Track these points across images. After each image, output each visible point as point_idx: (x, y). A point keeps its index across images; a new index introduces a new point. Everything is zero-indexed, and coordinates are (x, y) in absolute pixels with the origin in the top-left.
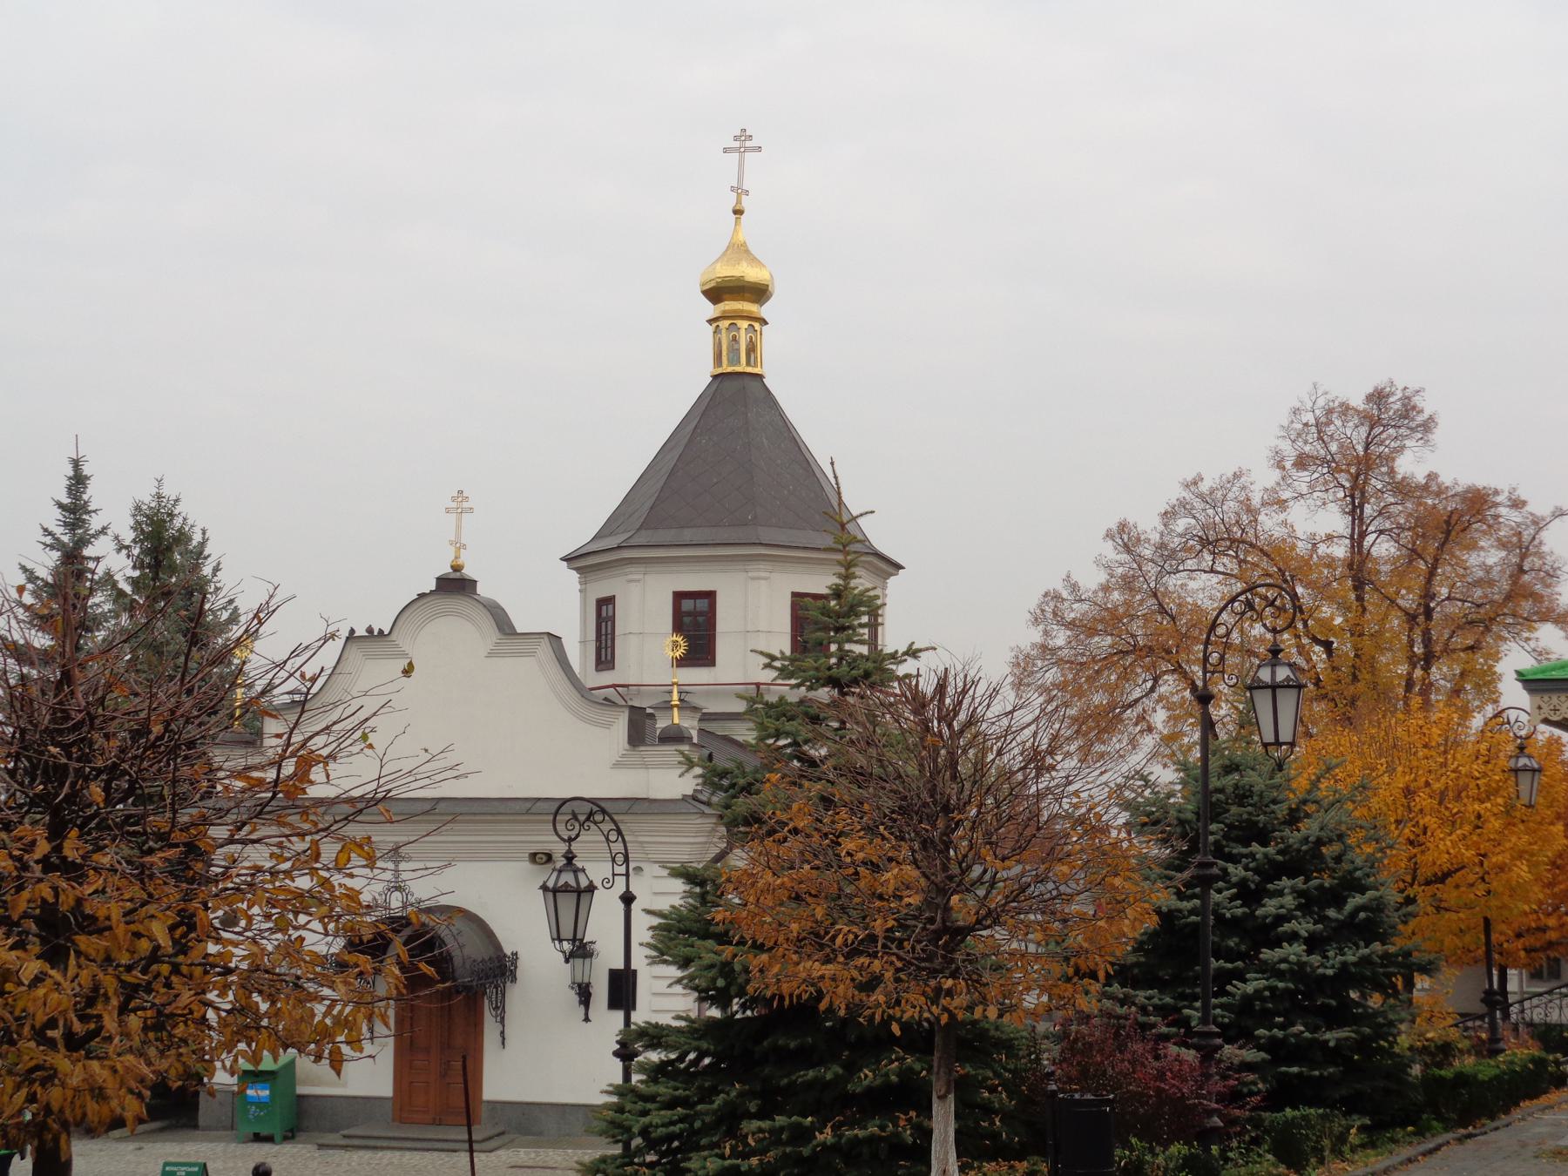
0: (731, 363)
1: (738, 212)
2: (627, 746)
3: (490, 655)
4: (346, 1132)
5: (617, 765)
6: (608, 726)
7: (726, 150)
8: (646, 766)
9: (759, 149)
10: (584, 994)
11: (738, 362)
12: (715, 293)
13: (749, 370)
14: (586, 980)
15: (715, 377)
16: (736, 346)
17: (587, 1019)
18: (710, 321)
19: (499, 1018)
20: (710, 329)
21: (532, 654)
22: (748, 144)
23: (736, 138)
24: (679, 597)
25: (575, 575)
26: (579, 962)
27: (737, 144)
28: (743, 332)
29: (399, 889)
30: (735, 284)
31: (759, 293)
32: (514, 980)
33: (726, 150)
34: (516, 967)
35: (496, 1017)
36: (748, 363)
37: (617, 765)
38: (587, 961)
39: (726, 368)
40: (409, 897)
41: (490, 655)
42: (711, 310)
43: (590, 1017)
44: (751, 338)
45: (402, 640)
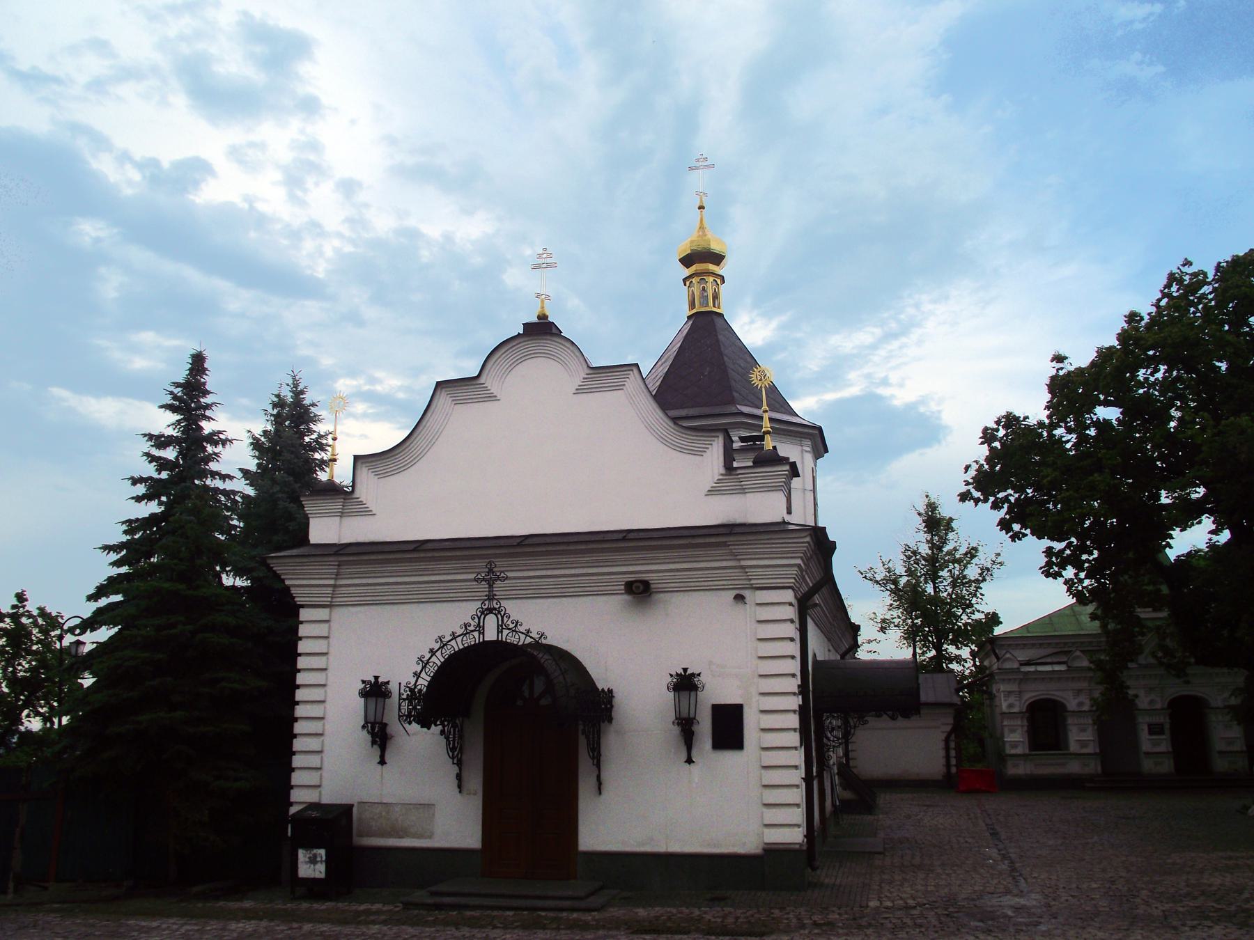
0: (702, 305)
1: (701, 207)
2: (722, 471)
3: (579, 391)
4: (434, 889)
5: (712, 492)
6: (700, 453)
8: (743, 491)
10: (686, 726)
11: (707, 305)
12: (687, 261)
13: (715, 310)
14: (692, 715)
15: (689, 318)
16: (705, 294)
17: (689, 761)
18: (685, 280)
19: (595, 761)
21: (620, 387)
22: (706, 163)
26: (684, 695)
28: (710, 285)
29: (491, 610)
30: (704, 253)
31: (718, 259)
32: (610, 720)
34: (612, 706)
35: (593, 758)
36: (714, 306)
37: (712, 492)
40: (505, 619)
41: (579, 391)
42: (687, 272)
44: (715, 289)
45: (489, 381)
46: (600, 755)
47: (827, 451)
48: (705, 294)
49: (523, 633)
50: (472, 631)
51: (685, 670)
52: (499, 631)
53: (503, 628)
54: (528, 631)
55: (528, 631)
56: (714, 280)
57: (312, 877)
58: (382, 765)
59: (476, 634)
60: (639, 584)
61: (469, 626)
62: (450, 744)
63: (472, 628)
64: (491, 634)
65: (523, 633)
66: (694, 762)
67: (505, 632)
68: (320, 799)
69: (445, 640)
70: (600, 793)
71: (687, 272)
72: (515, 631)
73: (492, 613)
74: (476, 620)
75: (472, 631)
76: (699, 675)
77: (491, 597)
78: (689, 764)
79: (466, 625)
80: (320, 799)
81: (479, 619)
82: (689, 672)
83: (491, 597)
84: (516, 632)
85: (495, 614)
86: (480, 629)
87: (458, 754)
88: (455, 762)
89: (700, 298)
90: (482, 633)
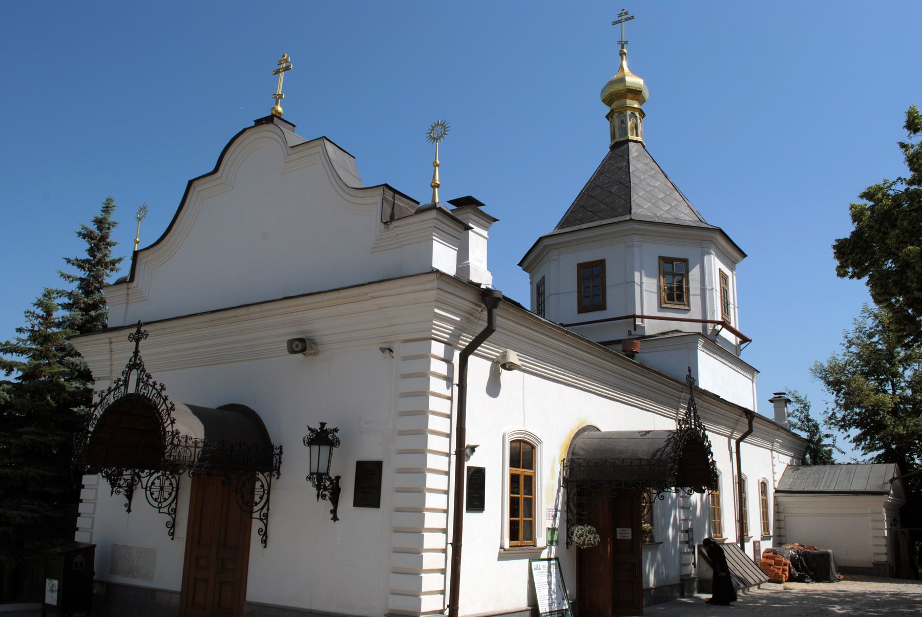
0: (621, 136)
7: (615, 23)
9: (632, 18)
11: (626, 134)
12: (609, 100)
16: (624, 126)
17: (335, 518)
18: (607, 117)
20: (608, 123)
23: (620, 15)
24: (581, 267)
25: (527, 275)
26: (315, 448)
27: (620, 18)
33: (615, 23)
38: (325, 449)
39: (617, 140)
43: (338, 516)
46: (268, 509)
47: (744, 255)
48: (624, 126)
49: (151, 386)
50: (121, 385)
51: (323, 425)
52: (138, 385)
53: (140, 382)
54: (155, 383)
55: (155, 383)
56: (632, 113)
57: (51, 603)
58: (129, 513)
59: (123, 388)
60: (297, 342)
61: (120, 381)
62: (152, 494)
63: (121, 383)
64: (132, 389)
65: (151, 386)
66: (338, 520)
67: (141, 384)
68: (91, 540)
69: (104, 394)
70: (265, 547)
71: (607, 110)
72: (146, 384)
73: (135, 368)
74: (125, 376)
75: (121, 385)
76: (336, 430)
77: (136, 353)
78: (335, 521)
79: (119, 380)
80: (91, 540)
81: (127, 374)
82: (327, 427)
83: (136, 353)
84: (148, 385)
85: (137, 370)
86: (126, 383)
87: (170, 504)
88: (165, 510)
89: (619, 130)
90: (126, 386)
